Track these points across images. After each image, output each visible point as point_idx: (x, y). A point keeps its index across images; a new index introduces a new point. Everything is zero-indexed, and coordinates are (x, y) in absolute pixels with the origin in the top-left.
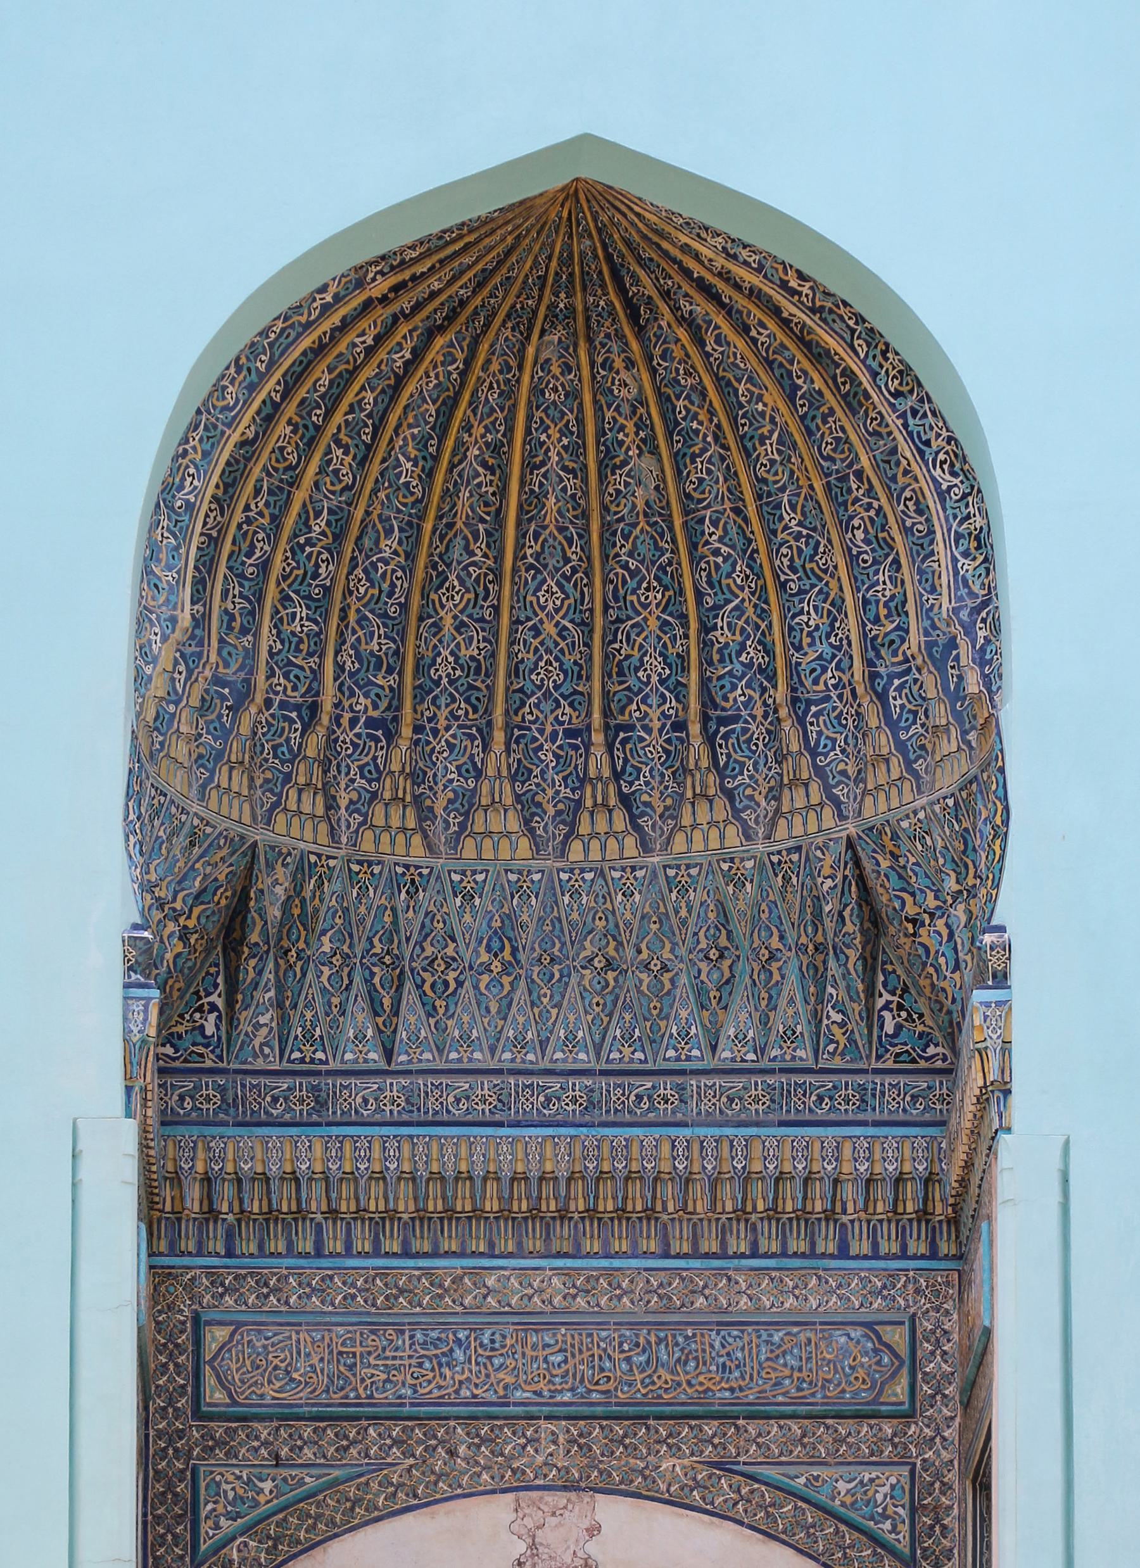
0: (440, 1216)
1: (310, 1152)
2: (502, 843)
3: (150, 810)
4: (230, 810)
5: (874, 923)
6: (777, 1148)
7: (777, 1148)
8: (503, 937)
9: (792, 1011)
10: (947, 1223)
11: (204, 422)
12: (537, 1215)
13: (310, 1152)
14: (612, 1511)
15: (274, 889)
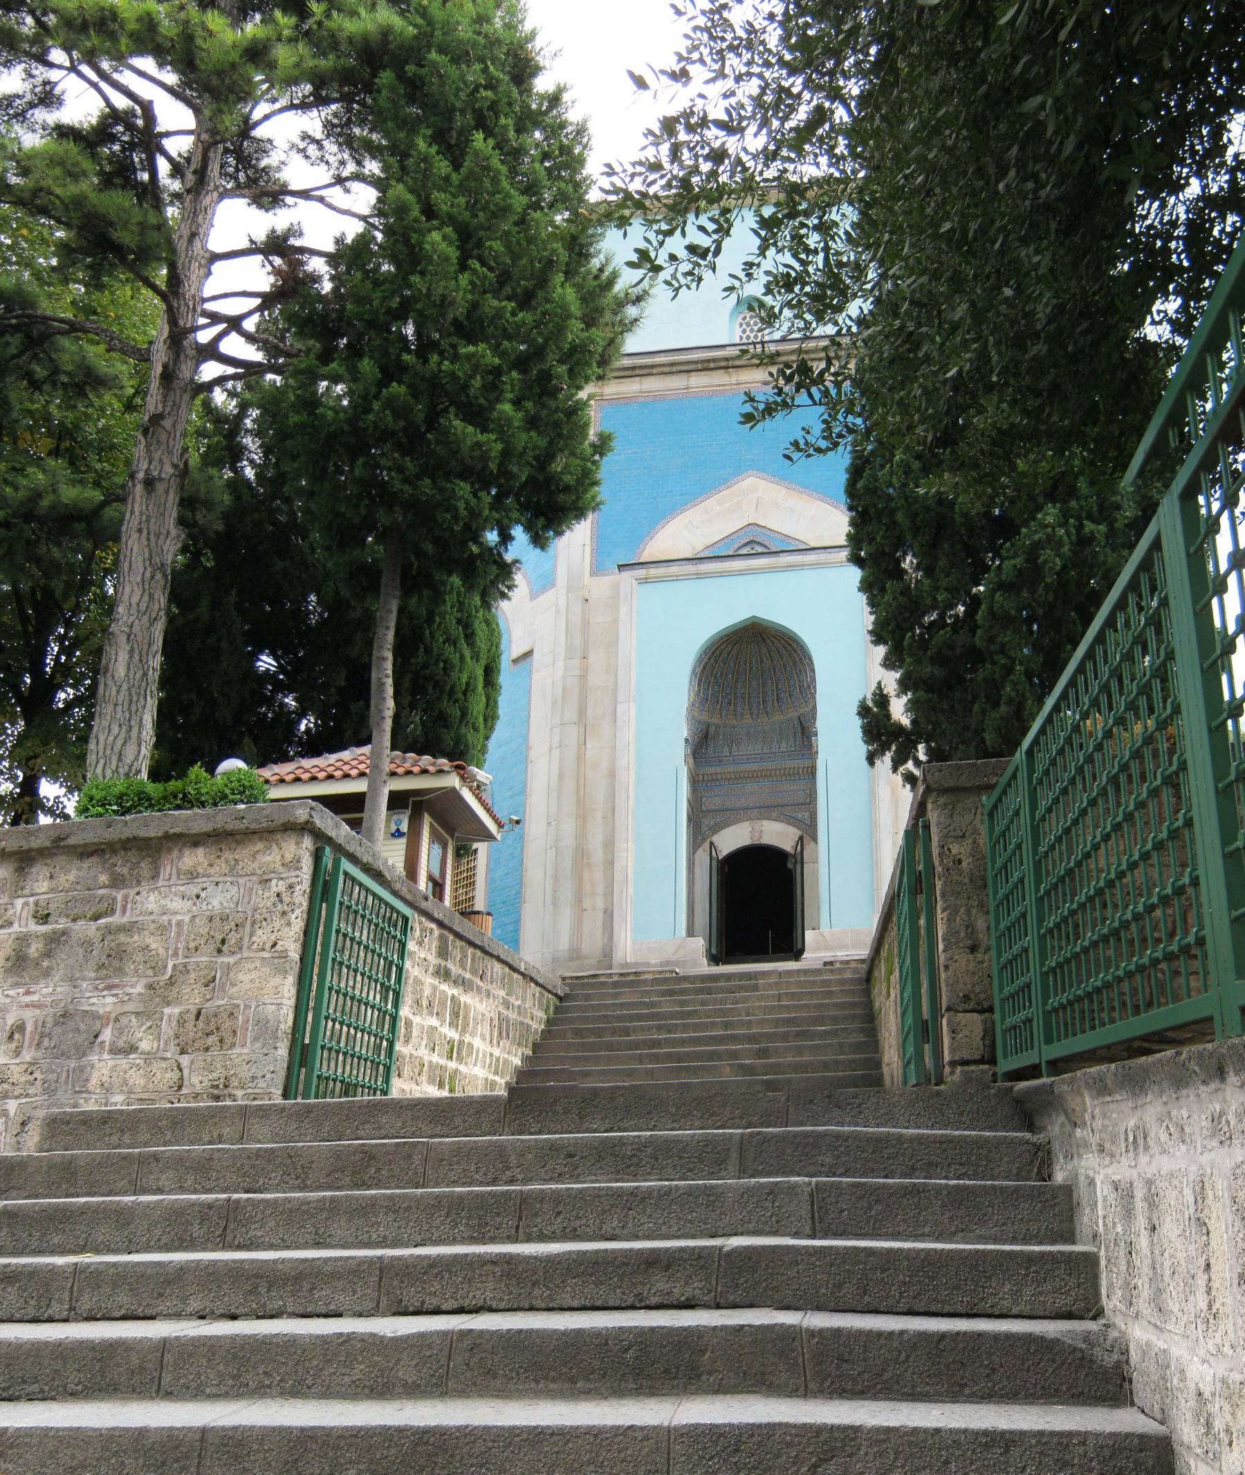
0: (740, 778)
1: (719, 770)
2: (748, 720)
3: (692, 720)
4: (705, 718)
5: (803, 728)
6: (791, 764)
7: (791, 764)
8: (748, 734)
9: (791, 742)
10: (812, 772)
11: (700, 660)
12: (754, 776)
13: (719, 770)
14: (765, 823)
15: (712, 729)
